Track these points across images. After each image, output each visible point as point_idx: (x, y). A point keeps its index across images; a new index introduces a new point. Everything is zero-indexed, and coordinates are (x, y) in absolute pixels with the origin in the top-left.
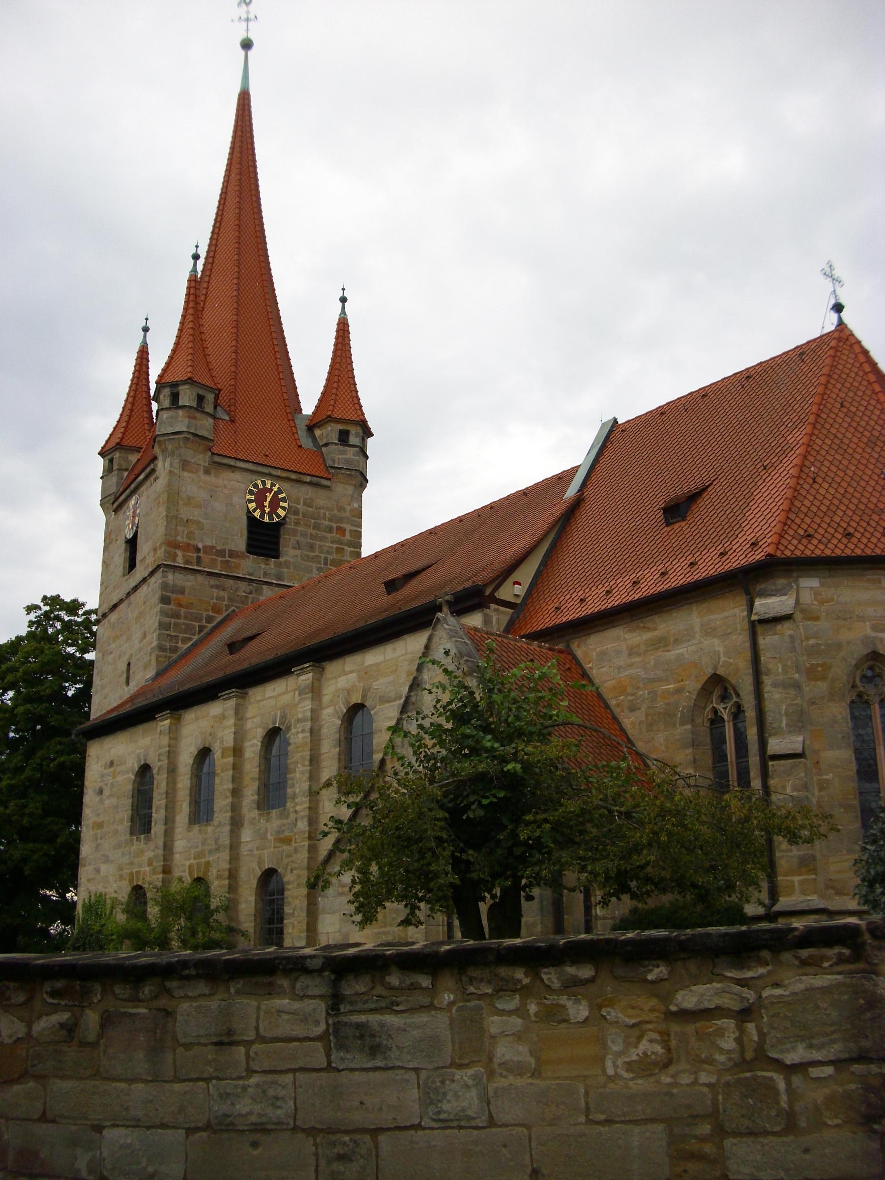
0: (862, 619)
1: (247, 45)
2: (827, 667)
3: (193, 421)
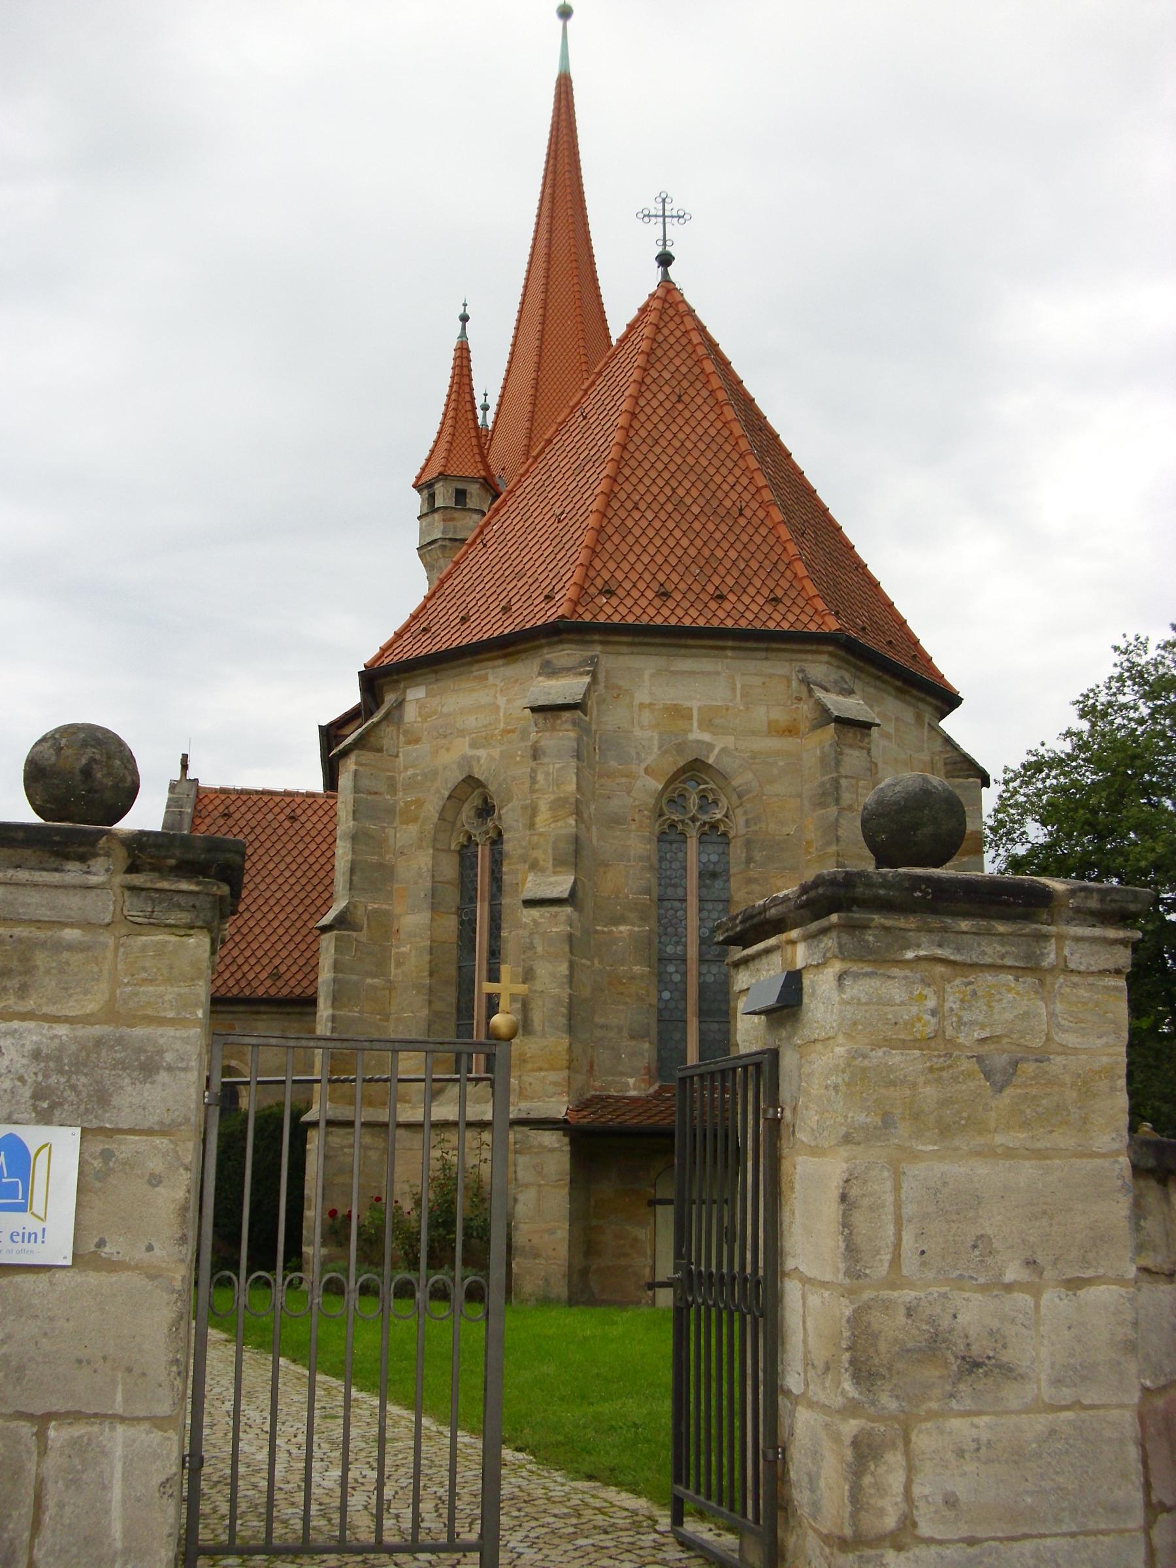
0: (462, 733)
2: (419, 803)
3: (451, 524)
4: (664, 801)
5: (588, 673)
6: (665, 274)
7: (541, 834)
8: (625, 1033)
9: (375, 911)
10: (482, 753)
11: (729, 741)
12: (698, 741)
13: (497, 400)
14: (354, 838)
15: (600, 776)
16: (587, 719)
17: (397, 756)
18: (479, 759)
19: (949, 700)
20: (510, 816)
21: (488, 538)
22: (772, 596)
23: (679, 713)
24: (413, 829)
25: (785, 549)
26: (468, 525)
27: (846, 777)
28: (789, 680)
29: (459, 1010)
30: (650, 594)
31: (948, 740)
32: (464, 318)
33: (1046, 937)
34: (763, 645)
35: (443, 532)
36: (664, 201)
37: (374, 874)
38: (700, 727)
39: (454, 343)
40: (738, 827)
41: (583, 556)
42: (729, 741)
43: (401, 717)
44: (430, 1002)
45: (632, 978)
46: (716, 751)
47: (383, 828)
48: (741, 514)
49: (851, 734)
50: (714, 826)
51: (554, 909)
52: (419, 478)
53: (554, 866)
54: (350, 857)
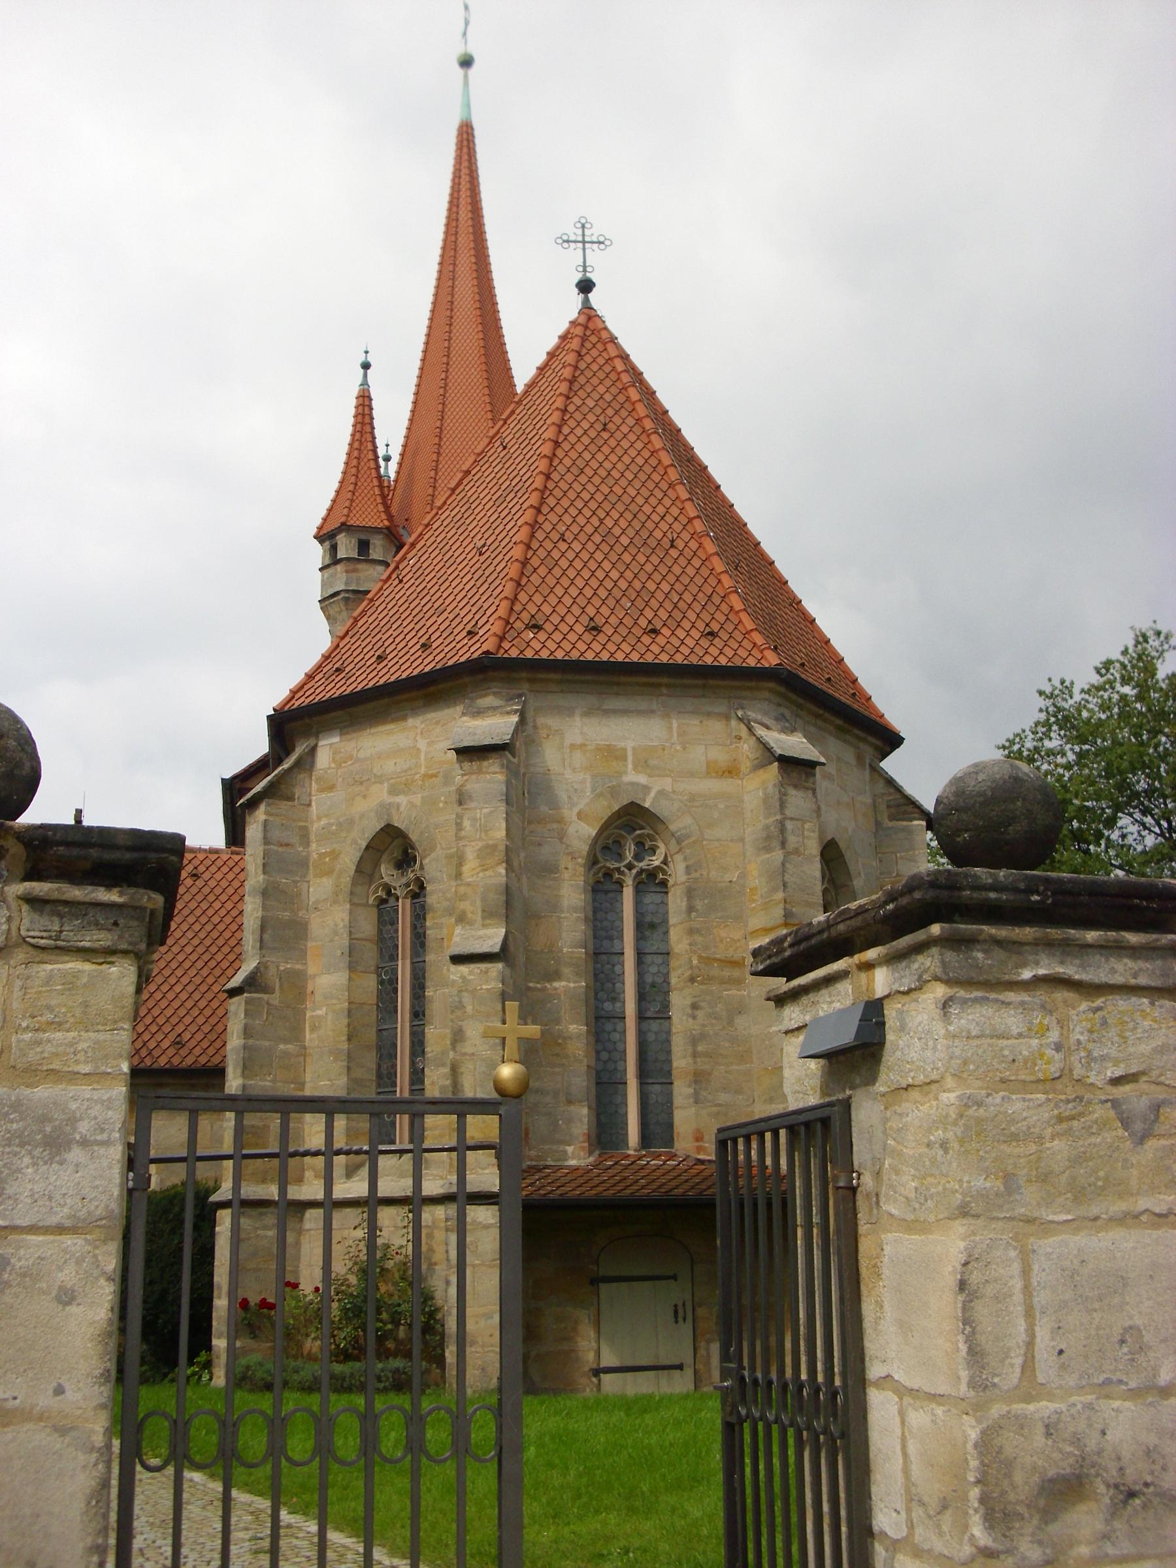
0: (380, 779)
1: (466, 62)
2: (334, 855)
3: (354, 575)
4: (598, 849)
5: (516, 711)
6: (586, 301)
7: (468, 884)
9: (287, 971)
10: (402, 800)
11: (667, 783)
12: (633, 784)
13: (399, 449)
14: (265, 893)
16: (515, 761)
17: (309, 805)
18: (398, 806)
19: (891, 740)
20: (433, 866)
21: (404, 573)
22: (708, 630)
23: (612, 753)
25: (719, 581)
26: (370, 577)
27: (792, 819)
29: (379, 1076)
30: (579, 629)
31: (890, 782)
32: (366, 366)
34: (699, 682)
35: (347, 584)
36: (583, 227)
37: (283, 931)
38: (635, 768)
39: (355, 391)
40: (678, 873)
41: (509, 590)
42: (667, 783)
44: (349, 1068)
46: (652, 794)
48: (672, 546)
50: (652, 874)
51: (483, 966)
52: (320, 528)
53: (483, 918)
54: (260, 914)
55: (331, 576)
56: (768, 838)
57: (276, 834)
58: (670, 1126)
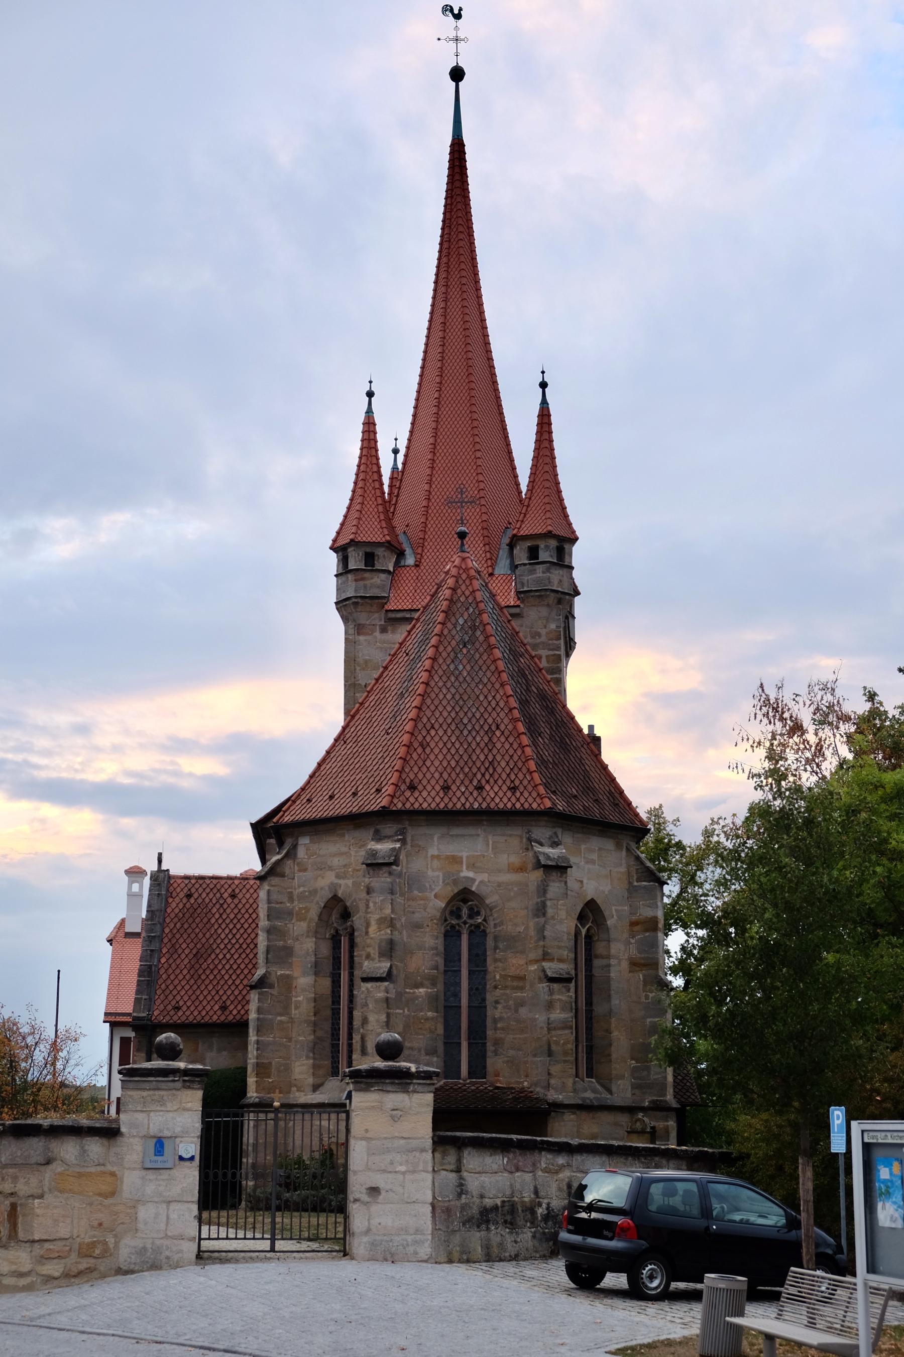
0: (331, 868)
1: (457, 74)
2: (307, 910)
3: (362, 583)
4: (447, 912)
5: (398, 840)
7: (372, 938)
8: (423, 1052)
9: (281, 975)
10: (341, 882)
11: (484, 877)
12: (465, 877)
13: (405, 442)
14: (269, 931)
15: (408, 900)
16: (399, 868)
17: (294, 879)
20: (357, 921)
21: (348, 736)
22: (512, 785)
23: (455, 860)
24: (304, 925)
25: (523, 752)
26: (376, 583)
28: (521, 837)
29: (333, 1035)
30: (438, 788)
32: (370, 394)
33: (410, 1084)
35: (356, 591)
37: (281, 954)
38: (467, 868)
39: (362, 417)
41: (398, 764)
42: (484, 877)
43: (295, 855)
44: (315, 1031)
45: (427, 1019)
46: (477, 883)
47: (286, 924)
49: (554, 875)
50: (478, 926)
51: (378, 984)
52: (334, 541)
53: (379, 957)
54: (266, 943)
55: (344, 583)
56: (538, 910)
57: (274, 897)
58: (485, 1067)
